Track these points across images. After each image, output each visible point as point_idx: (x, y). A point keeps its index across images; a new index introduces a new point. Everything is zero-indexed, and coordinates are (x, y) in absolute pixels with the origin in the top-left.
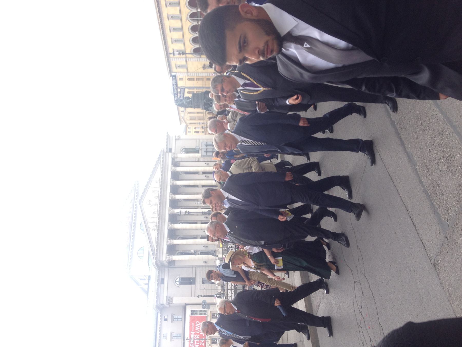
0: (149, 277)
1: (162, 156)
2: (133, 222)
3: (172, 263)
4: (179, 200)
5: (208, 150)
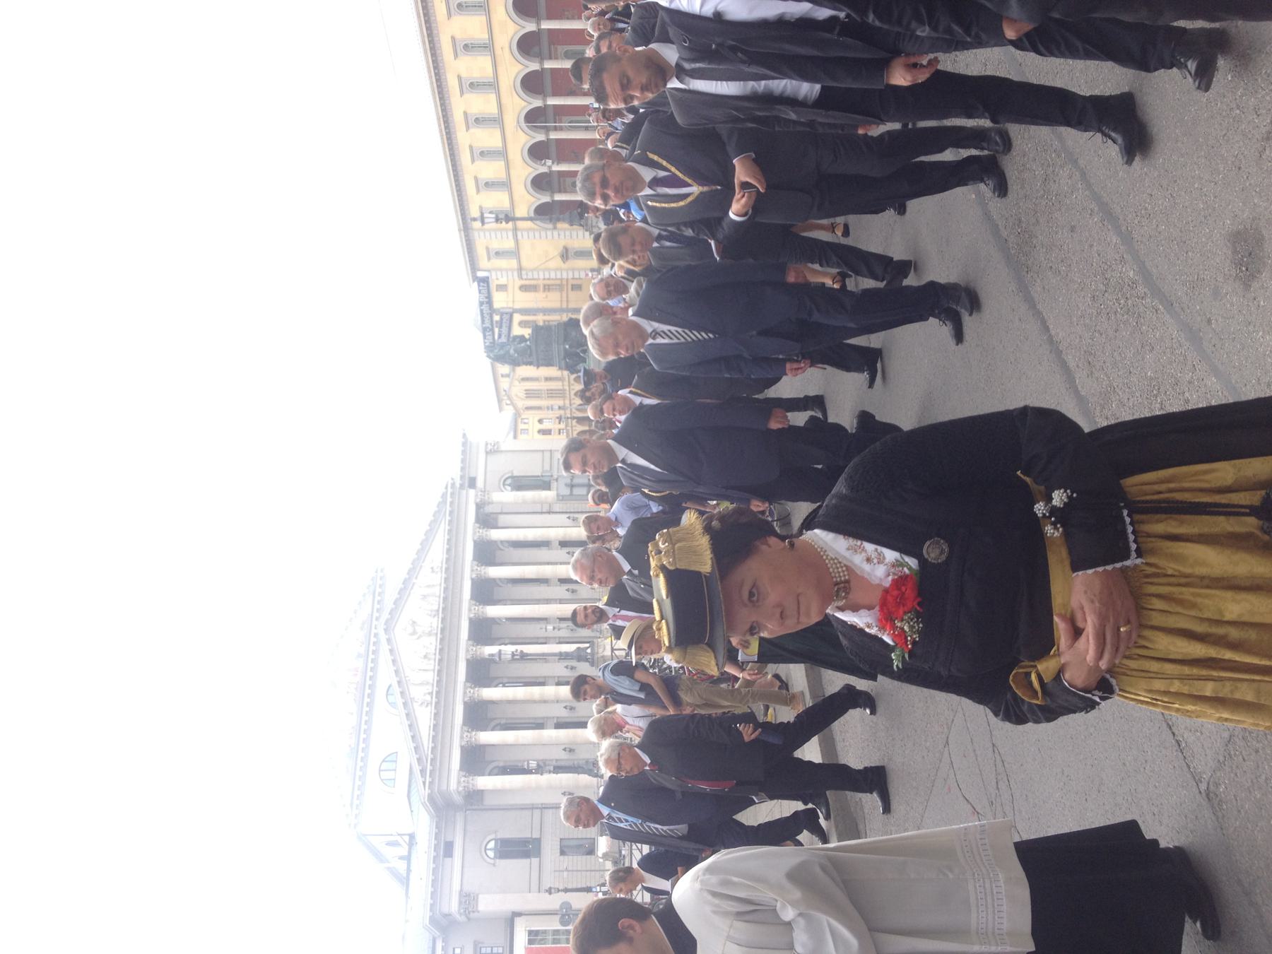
0: (412, 836)
1: (449, 499)
2: (369, 682)
3: (474, 798)
4: (494, 621)
5: (576, 481)
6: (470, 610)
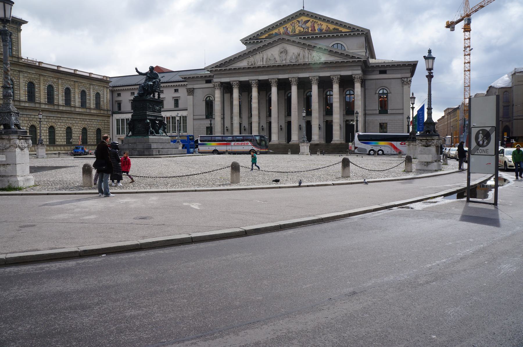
6: (293, 78)
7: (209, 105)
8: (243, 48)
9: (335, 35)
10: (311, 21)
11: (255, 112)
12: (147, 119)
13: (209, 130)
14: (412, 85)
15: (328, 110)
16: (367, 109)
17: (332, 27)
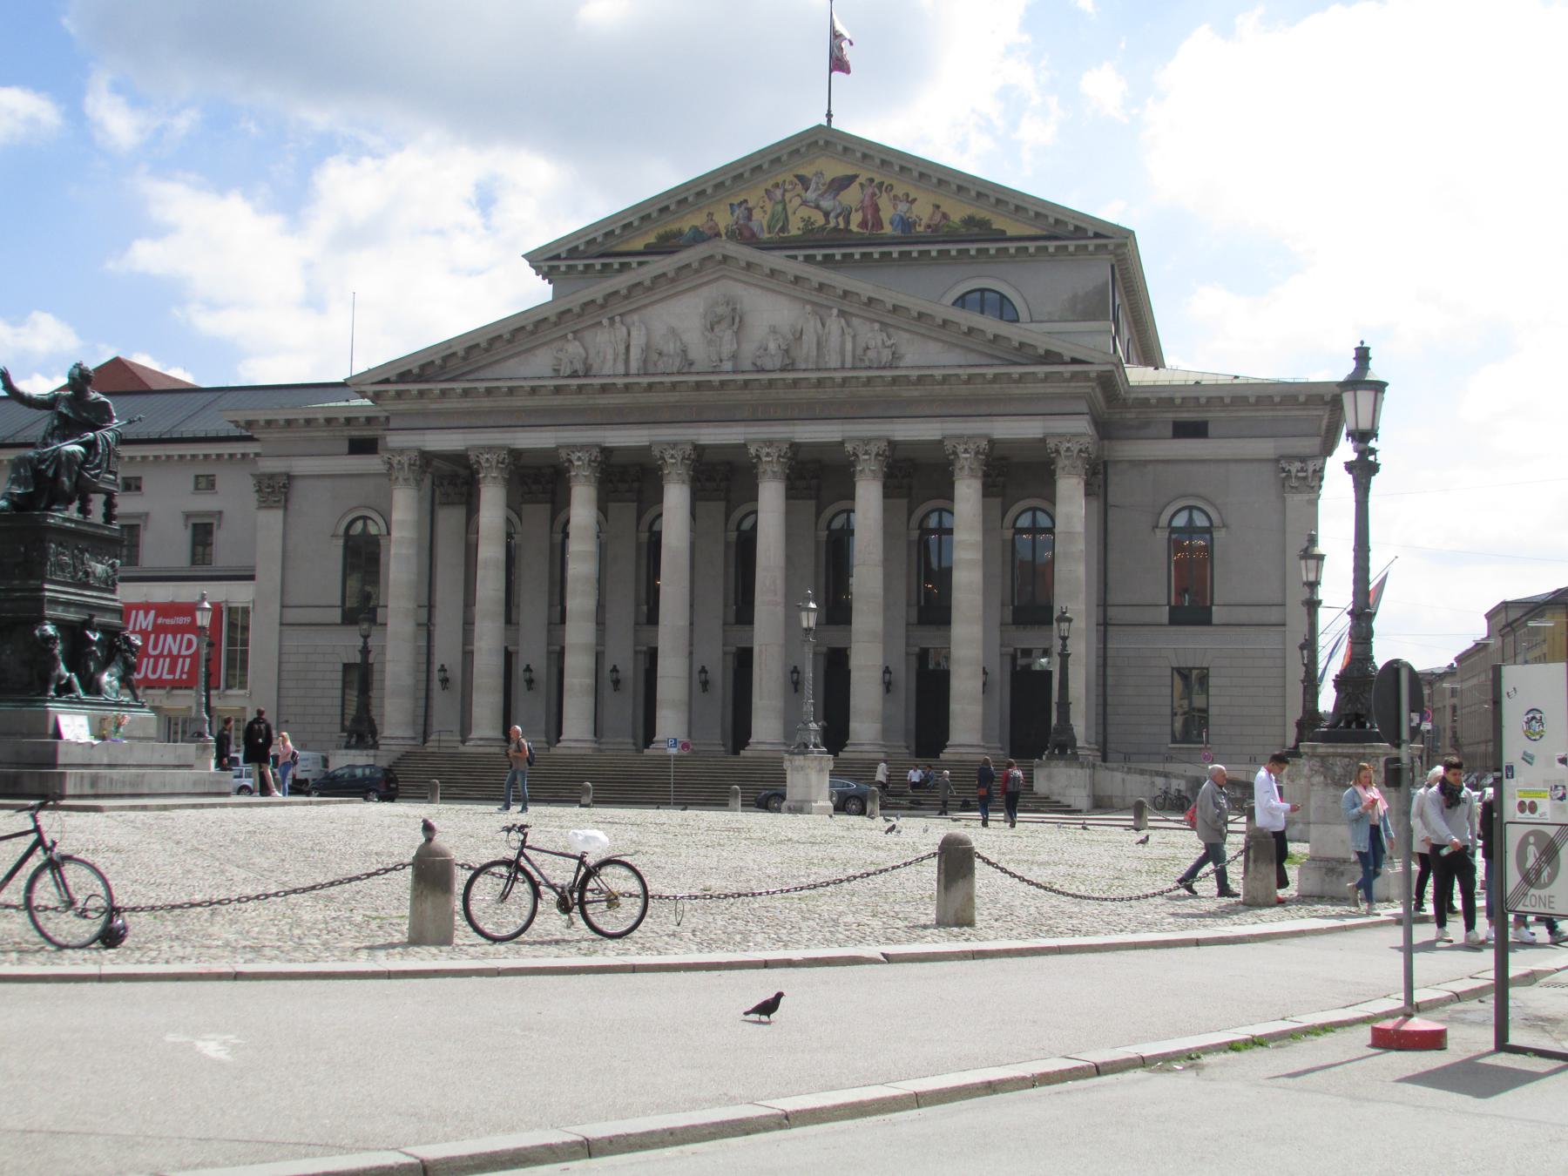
1: (1041, 370)
6: (770, 443)
7: (363, 556)
8: (537, 291)
9: (973, 248)
10: (862, 179)
11: (580, 601)
12: (41, 620)
13: (355, 676)
14: (1322, 492)
15: (930, 604)
16: (1112, 599)
17: (958, 212)
